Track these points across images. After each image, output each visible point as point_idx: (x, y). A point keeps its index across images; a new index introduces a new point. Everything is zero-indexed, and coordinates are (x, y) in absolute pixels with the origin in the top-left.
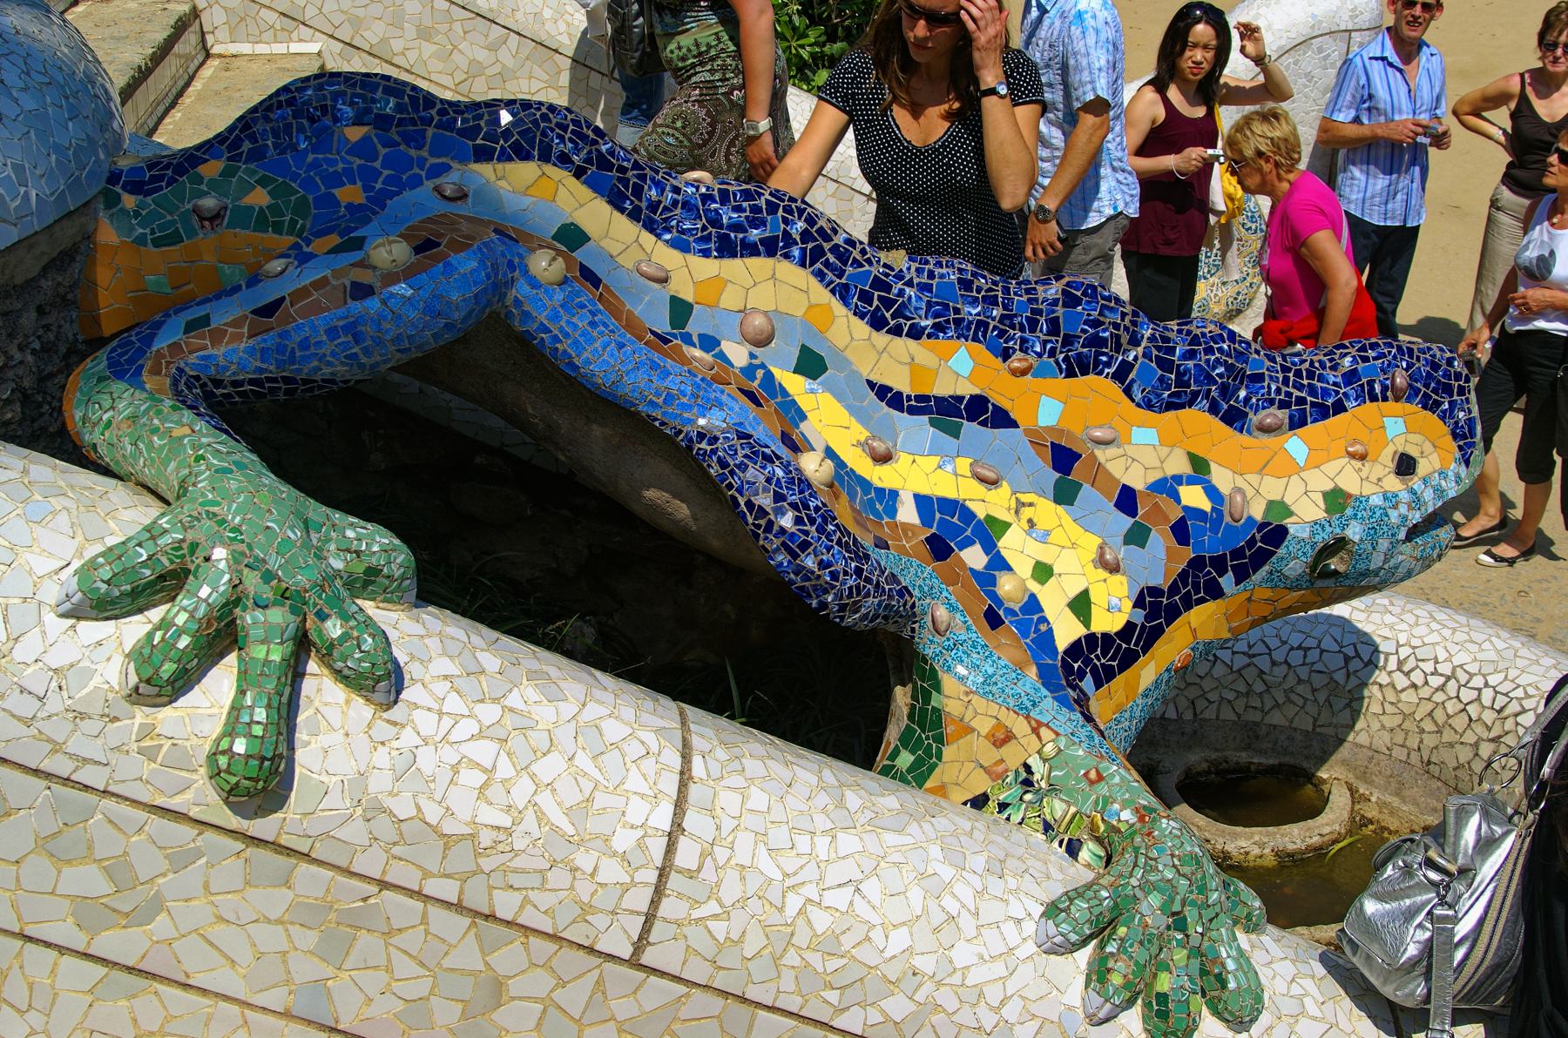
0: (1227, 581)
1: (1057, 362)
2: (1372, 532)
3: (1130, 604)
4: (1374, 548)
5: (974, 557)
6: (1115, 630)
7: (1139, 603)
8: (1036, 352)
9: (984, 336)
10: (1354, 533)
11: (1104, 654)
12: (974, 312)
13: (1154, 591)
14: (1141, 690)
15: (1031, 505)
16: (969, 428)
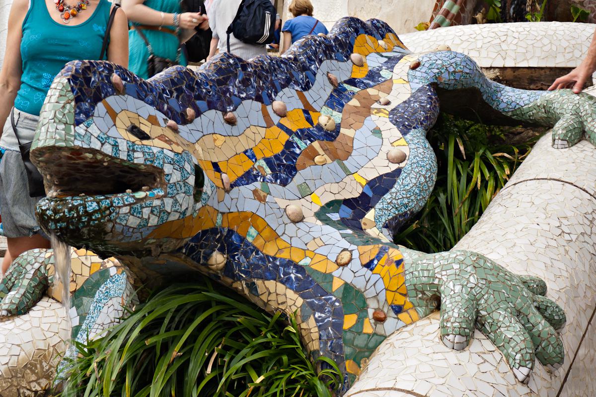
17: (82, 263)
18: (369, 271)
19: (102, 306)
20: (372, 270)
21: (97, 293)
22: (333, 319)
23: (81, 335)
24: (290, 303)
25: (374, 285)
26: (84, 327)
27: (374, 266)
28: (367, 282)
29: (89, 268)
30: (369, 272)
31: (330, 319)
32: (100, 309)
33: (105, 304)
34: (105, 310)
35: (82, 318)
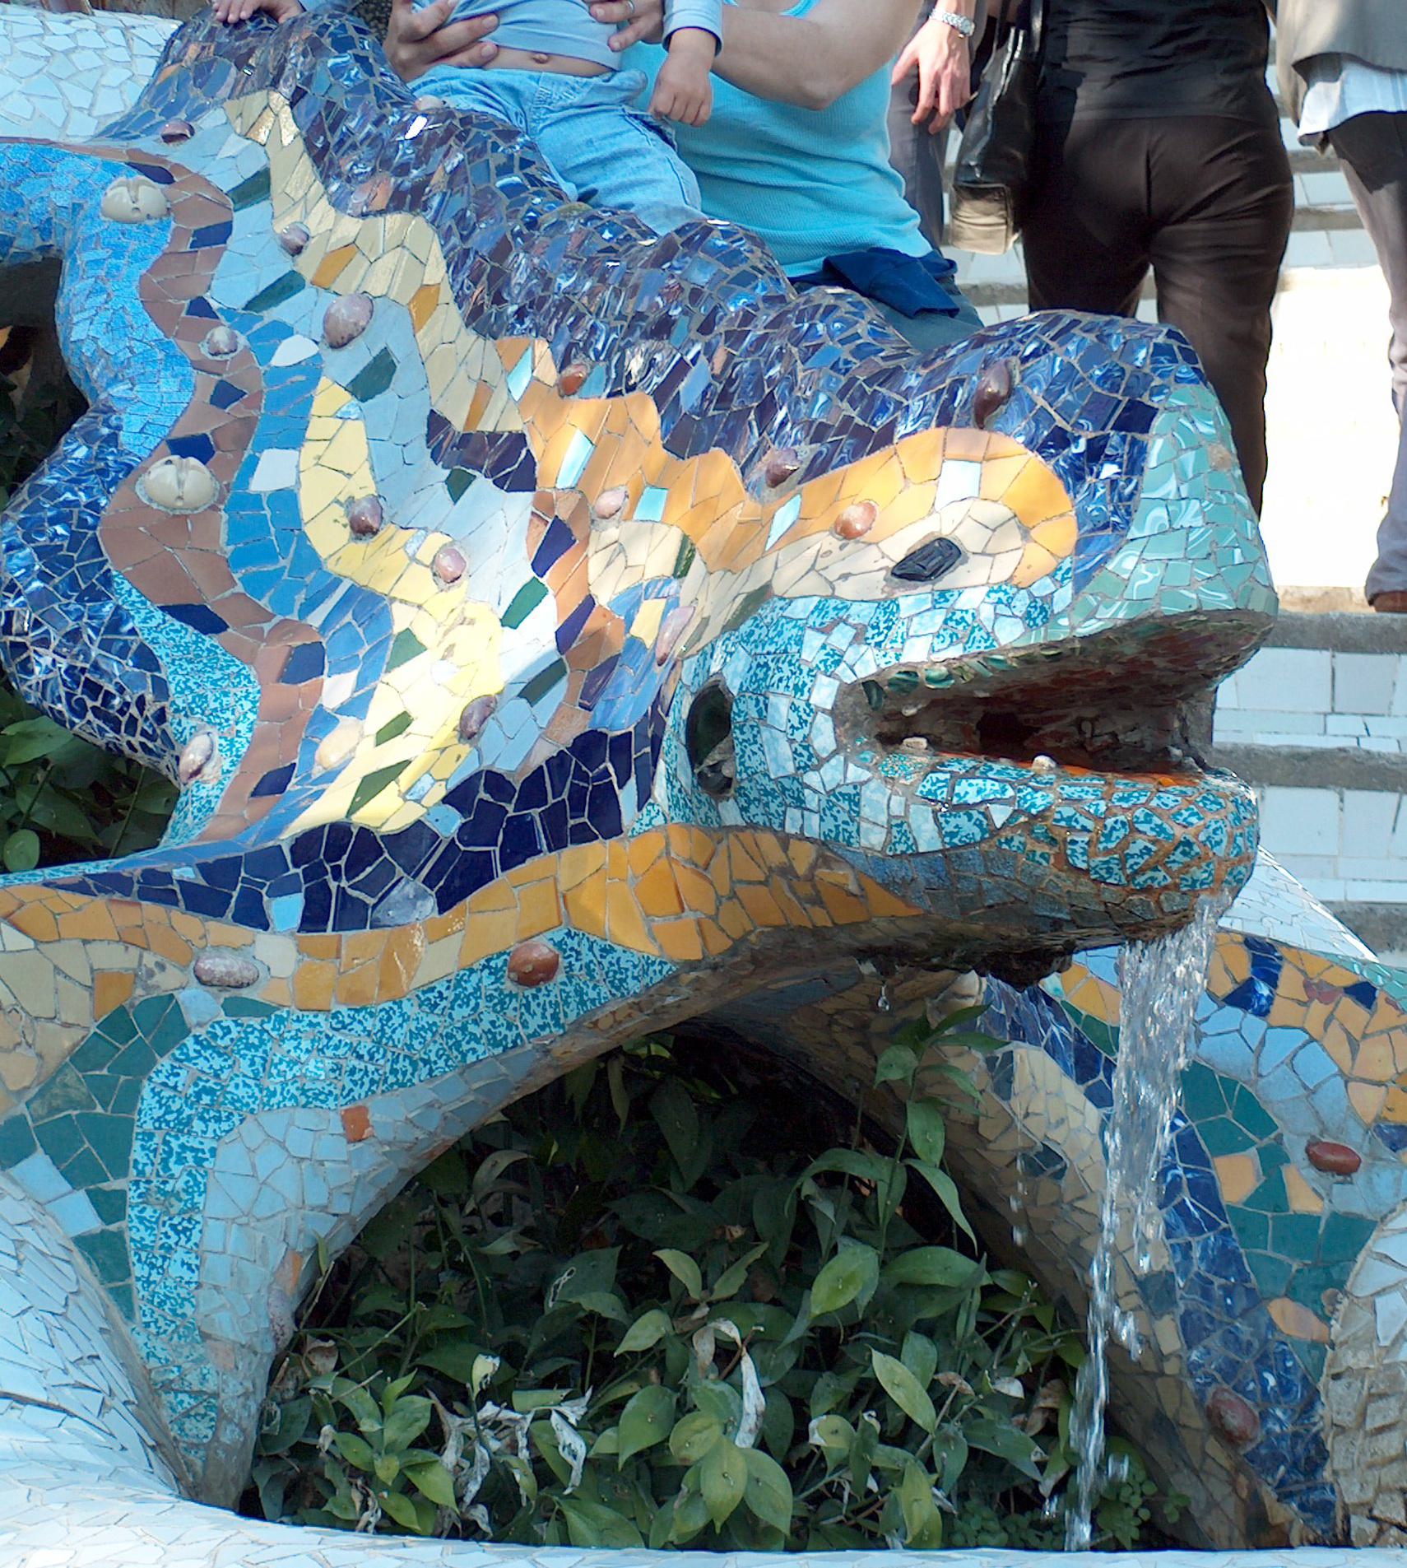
0: (627, 796)
1: (608, 369)
2: (761, 675)
3: (443, 793)
4: (759, 712)
5: (336, 688)
6: (388, 828)
7: (458, 797)
8: (595, 351)
9: (557, 326)
10: (735, 673)
11: (353, 869)
12: (565, 284)
13: (495, 781)
14: (421, 979)
15: (472, 622)
16: (482, 485)
17: (57, 970)
18: (1251, 1017)
19: (206, 1147)
20: (1263, 1013)
21: (146, 1092)
22: (1186, 1170)
23: (152, 1266)
24: (1074, 1120)
25: (1291, 1061)
26: (135, 1231)
27: (1264, 1001)
28: (1258, 1053)
29: (86, 994)
30: (1253, 1025)
31: (1180, 1172)
32: (199, 1162)
33: (218, 1138)
34: (231, 1158)
35: (110, 1206)
